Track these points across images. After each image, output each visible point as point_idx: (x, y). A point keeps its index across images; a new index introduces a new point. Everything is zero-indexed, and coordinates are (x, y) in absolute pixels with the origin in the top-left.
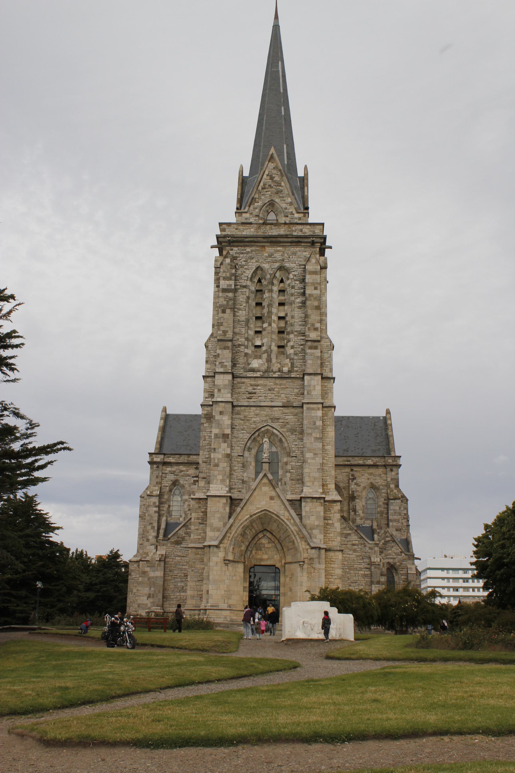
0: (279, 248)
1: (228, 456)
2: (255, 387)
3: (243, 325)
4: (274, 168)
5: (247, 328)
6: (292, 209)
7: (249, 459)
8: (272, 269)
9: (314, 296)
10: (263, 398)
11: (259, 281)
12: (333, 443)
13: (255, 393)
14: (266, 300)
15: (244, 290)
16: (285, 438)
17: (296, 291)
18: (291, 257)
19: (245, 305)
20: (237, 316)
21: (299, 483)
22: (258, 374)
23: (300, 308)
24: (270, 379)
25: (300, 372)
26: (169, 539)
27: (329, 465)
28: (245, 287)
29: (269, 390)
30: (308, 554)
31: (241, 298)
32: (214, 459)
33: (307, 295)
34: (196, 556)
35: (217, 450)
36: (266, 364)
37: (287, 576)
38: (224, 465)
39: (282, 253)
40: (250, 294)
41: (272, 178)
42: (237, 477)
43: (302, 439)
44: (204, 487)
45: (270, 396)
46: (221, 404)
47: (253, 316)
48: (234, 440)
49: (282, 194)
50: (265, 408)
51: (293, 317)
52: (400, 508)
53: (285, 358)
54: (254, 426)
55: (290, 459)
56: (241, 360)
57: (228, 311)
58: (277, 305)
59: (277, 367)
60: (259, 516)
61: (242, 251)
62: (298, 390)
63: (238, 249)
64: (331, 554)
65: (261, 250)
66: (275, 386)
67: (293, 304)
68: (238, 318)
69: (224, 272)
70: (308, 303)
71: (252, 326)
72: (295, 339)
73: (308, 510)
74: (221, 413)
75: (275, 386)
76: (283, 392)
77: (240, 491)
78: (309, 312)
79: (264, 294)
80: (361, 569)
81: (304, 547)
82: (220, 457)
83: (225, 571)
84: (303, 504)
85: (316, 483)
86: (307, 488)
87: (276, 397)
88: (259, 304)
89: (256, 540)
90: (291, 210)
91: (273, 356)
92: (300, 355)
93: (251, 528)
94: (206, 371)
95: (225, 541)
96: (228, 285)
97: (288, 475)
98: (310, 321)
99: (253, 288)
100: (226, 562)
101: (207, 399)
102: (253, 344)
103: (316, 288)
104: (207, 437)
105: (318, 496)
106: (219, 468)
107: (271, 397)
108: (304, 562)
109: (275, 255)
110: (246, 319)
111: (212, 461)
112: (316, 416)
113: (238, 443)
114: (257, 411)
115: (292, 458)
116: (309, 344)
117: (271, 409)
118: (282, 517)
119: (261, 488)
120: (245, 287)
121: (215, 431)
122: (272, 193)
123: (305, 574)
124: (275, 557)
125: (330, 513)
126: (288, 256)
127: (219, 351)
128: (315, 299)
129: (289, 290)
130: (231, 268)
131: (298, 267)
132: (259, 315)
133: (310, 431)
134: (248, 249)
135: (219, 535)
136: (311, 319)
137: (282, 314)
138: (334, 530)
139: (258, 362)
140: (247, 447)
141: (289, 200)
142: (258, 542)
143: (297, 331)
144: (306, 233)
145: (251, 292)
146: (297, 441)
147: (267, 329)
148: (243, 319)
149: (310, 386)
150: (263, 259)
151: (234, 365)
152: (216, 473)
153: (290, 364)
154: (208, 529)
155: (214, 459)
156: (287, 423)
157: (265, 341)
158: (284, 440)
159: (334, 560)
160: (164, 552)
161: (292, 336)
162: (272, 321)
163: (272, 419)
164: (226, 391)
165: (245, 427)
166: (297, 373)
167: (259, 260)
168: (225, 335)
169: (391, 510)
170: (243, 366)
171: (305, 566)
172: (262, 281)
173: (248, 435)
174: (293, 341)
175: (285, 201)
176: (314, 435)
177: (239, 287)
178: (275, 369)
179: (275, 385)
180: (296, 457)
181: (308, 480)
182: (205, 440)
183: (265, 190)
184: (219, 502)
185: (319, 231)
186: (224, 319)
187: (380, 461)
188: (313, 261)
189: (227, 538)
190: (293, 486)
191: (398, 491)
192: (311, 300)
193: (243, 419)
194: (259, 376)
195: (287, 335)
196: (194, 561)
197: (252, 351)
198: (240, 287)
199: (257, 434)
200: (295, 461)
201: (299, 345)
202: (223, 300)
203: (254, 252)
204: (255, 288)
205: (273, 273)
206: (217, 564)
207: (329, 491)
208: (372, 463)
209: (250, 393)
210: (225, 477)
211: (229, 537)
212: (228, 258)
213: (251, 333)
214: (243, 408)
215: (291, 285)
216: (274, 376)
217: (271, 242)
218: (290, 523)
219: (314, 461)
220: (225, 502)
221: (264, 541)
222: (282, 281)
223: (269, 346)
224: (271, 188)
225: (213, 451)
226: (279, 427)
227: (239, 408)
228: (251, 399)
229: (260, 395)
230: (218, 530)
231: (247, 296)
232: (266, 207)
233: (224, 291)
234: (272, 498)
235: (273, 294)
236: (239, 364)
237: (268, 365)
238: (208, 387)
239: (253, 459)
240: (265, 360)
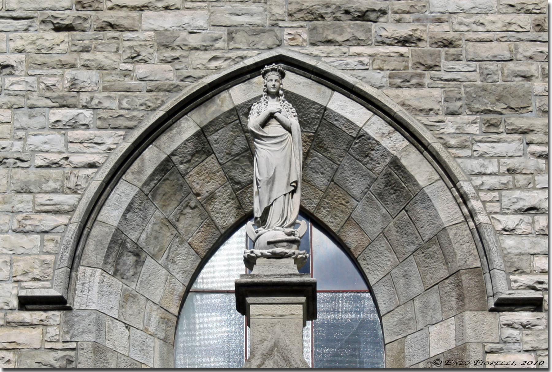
16: (436, 158)
156: (449, 44)
200: (530, 341)
226: (379, 77)
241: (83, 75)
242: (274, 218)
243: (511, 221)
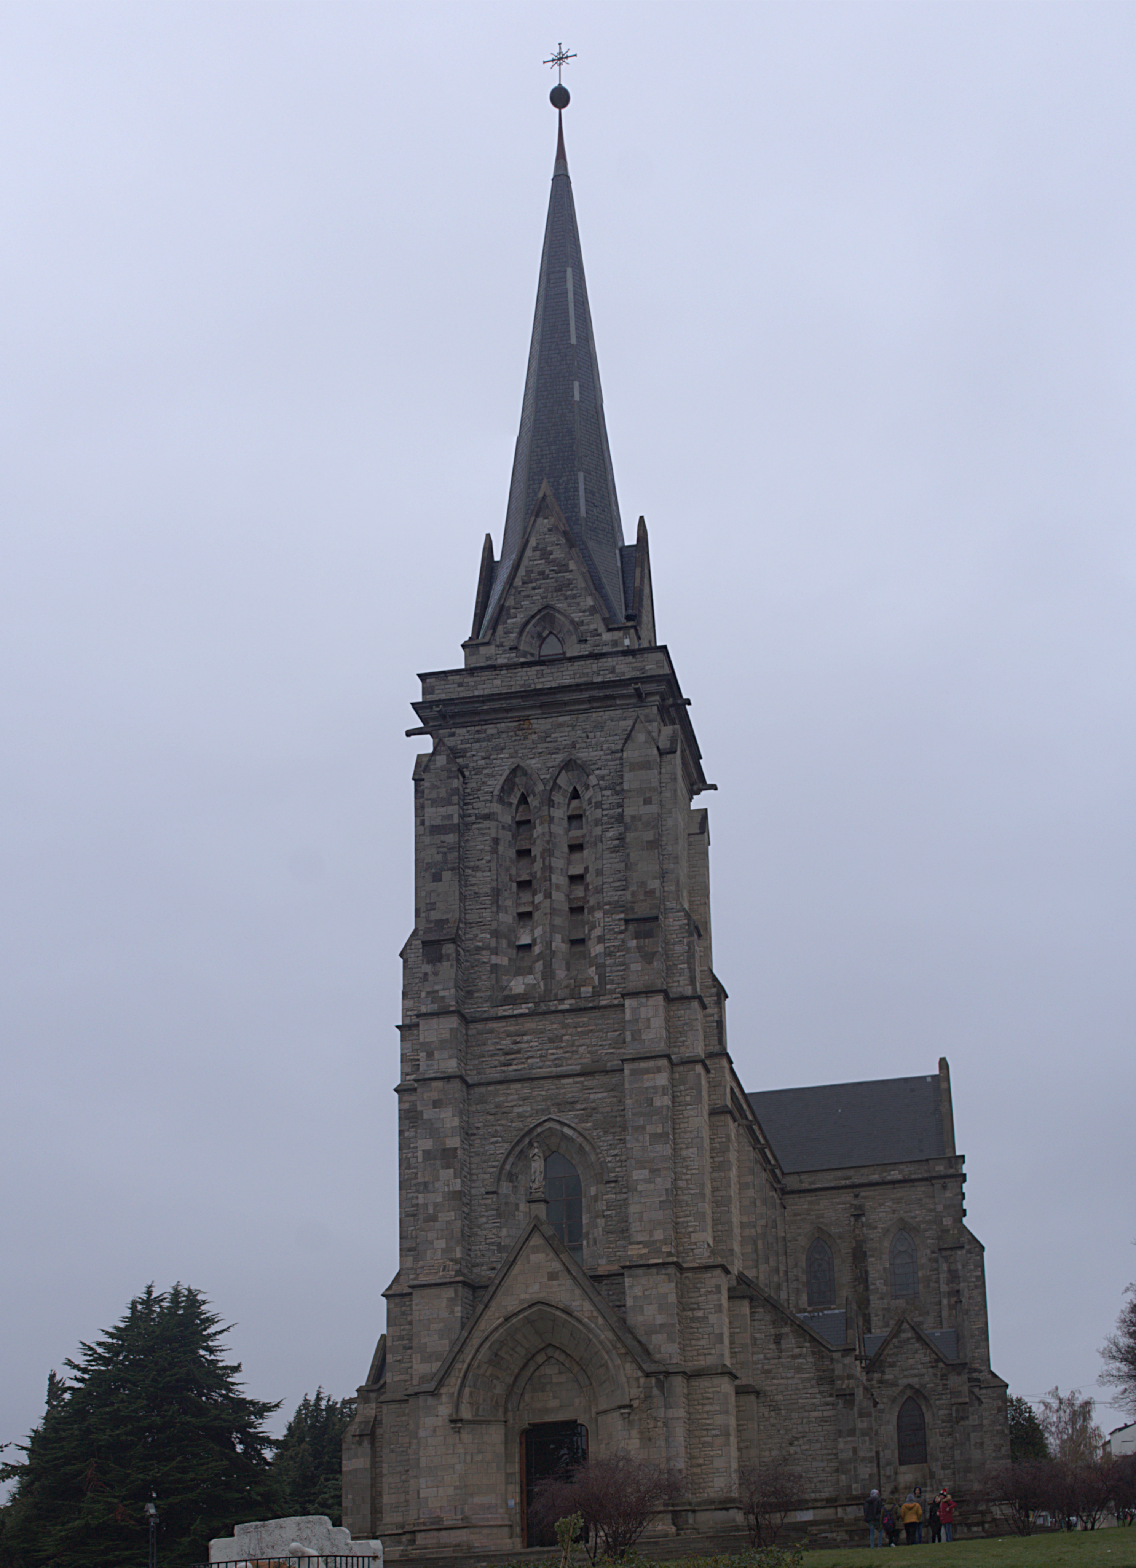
0: (561, 719)
1: (457, 1196)
2: (518, 1039)
5: (494, 909)
8: (549, 768)
10: (538, 1060)
11: (523, 799)
13: (518, 1052)
14: (538, 842)
15: (487, 823)
18: (591, 735)
19: (488, 858)
20: (471, 885)
22: (524, 1009)
24: (552, 1017)
27: (692, 1192)
28: (487, 817)
29: (551, 1040)
31: (479, 844)
38: (447, 1216)
40: (500, 831)
42: (486, 1239)
43: (623, 1141)
44: (412, 1268)
45: (553, 1054)
47: (511, 880)
48: (476, 1159)
50: (542, 1082)
54: (520, 1125)
56: (484, 982)
57: (447, 875)
62: (617, 1033)
64: (704, 1383)
66: (563, 1032)
68: (475, 888)
71: (509, 903)
72: (607, 920)
75: (563, 1032)
76: (582, 1042)
79: (535, 828)
84: (628, 1281)
86: (636, 1246)
87: (567, 1055)
88: (524, 853)
89: (532, 1369)
92: (618, 954)
94: (404, 1016)
96: (444, 818)
99: (507, 819)
101: (408, 1078)
102: (510, 944)
105: (660, 1261)
107: (553, 1057)
109: (553, 736)
110: (493, 889)
112: (655, 1087)
113: (484, 1165)
114: (525, 1090)
115: (608, 1185)
117: (557, 1082)
120: (487, 817)
124: (577, 1401)
126: (584, 735)
130: (449, 778)
131: (609, 757)
132: (525, 877)
133: (641, 1121)
139: (526, 981)
142: (537, 1374)
143: (608, 904)
145: (503, 828)
146: (619, 1146)
148: (487, 889)
149: (637, 1021)
150: (525, 748)
153: (596, 978)
156: (594, 1109)
157: (538, 932)
158: (587, 1148)
159: (711, 1396)
161: (599, 915)
162: (554, 887)
163: (558, 1104)
166: (614, 996)
167: (516, 752)
170: (489, 993)
172: (529, 800)
173: (506, 1145)
174: (602, 925)
176: (650, 1129)
177: (473, 818)
179: (563, 1028)
180: (616, 1181)
181: (639, 1229)
186: (438, 895)
193: (493, 1111)
194: (527, 1011)
195: (589, 914)
197: (510, 959)
199: (527, 1140)
201: (616, 933)
203: (504, 735)
204: (513, 818)
209: (507, 1054)
213: (507, 919)
214: (491, 1088)
216: (561, 1007)
217: (542, 706)
218: (596, 1324)
219: (651, 1186)
221: (549, 1370)
223: (547, 943)
226: (576, 1120)
227: (483, 1089)
228: (510, 1065)
233: (435, 830)
235: (552, 826)
236: (479, 991)
237: (546, 985)
238: (410, 1050)
240: (539, 976)
241: (498, 1128)
243: (609, 1159)
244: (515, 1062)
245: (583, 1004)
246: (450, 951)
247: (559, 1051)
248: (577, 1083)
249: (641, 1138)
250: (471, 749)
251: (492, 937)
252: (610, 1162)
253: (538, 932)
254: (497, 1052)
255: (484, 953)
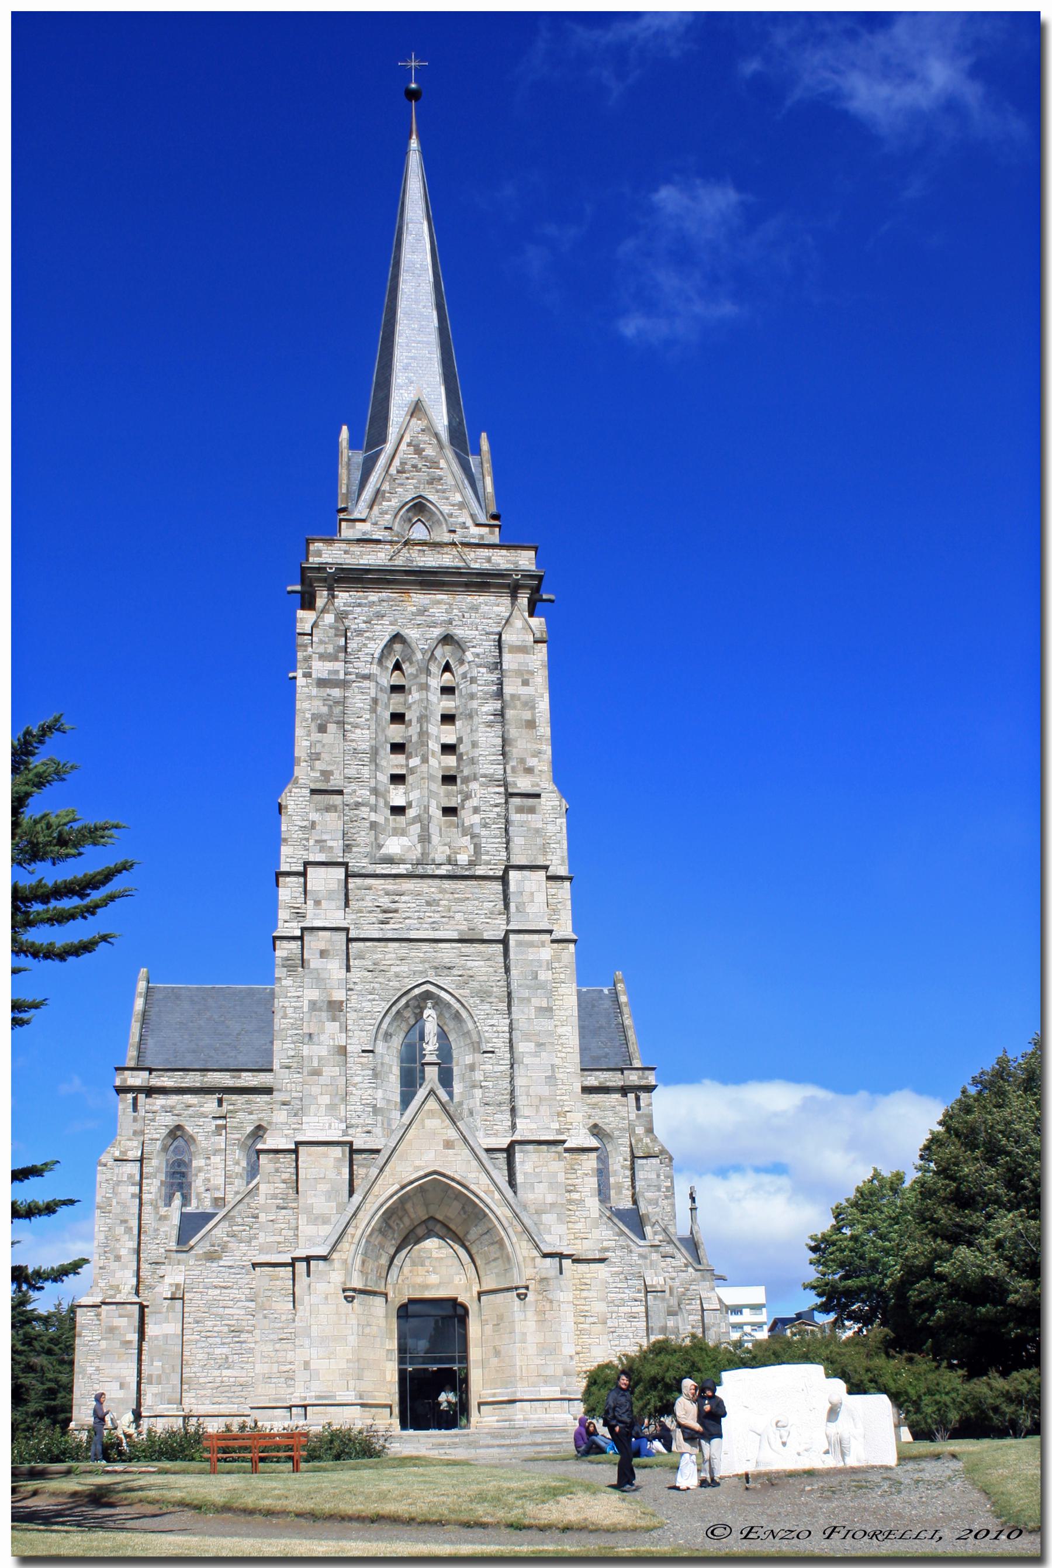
0: (439, 597)
2: (397, 898)
3: (366, 759)
4: (423, 430)
5: (373, 767)
6: (465, 518)
7: (387, 1059)
9: (523, 698)
10: (416, 921)
11: (397, 667)
12: (575, 1021)
13: (396, 911)
14: (414, 707)
15: (366, 684)
16: (468, 1010)
17: (480, 688)
19: (368, 717)
21: (502, 1112)
22: (402, 869)
23: (490, 725)
24: (430, 881)
25: (495, 864)
26: (192, 1248)
27: (568, 1071)
28: (367, 677)
29: (428, 904)
30: (535, 1270)
32: (311, 1057)
33: (507, 697)
34: (272, 1283)
35: (315, 1039)
36: (419, 846)
37: (487, 1321)
39: (447, 606)
41: (418, 451)
42: (361, 1099)
45: (430, 917)
46: (321, 933)
47: (386, 741)
49: (442, 485)
51: (474, 745)
52: (658, 1176)
53: (460, 835)
55: (479, 1057)
56: (363, 837)
57: (332, 728)
58: (439, 718)
59: (443, 853)
60: (420, 1185)
61: (359, 601)
62: (493, 904)
63: (350, 596)
65: (402, 599)
66: (441, 896)
67: (475, 717)
69: (321, 642)
70: (510, 713)
72: (483, 792)
73: (530, 1171)
74: (323, 954)
75: (441, 896)
77: (369, 1132)
78: (513, 732)
79: (410, 693)
80: (623, 1303)
81: (525, 1253)
82: (324, 1053)
83: (347, 1314)
84: (518, 1157)
85: (544, 1109)
88: (398, 718)
90: (461, 520)
91: (434, 829)
92: (493, 826)
93: (400, 1213)
95: (344, 1245)
97: (478, 1092)
98: (515, 752)
100: (350, 1294)
102: (386, 803)
103: (526, 683)
104: (290, 1011)
106: (322, 1080)
108: (527, 1288)
109: (431, 610)
111: (306, 1063)
112: (539, 961)
113: (361, 1022)
114: (402, 949)
116: (516, 801)
117: (434, 945)
118: (472, 1187)
119: (423, 1120)
120: (367, 677)
121: (312, 994)
122: (419, 482)
123: (530, 1314)
124: (456, 1279)
125: (574, 1176)
127: (314, 816)
128: (525, 704)
129: (463, 687)
130: (336, 635)
132: (398, 740)
133: (526, 993)
134: (373, 597)
135: (327, 1232)
136: (517, 747)
137: (451, 740)
138: (585, 1214)
140: (382, 1031)
141: (458, 498)
143: (485, 776)
144: (499, 565)
145: (381, 690)
146: (495, 1017)
147: (418, 770)
148: (365, 746)
149: (521, 893)
150: (404, 618)
151: (347, 848)
152: (315, 1090)
154: (303, 1219)
155: (311, 1057)
157: (414, 796)
158: (464, 1014)
159: (588, 1281)
160: (180, 1279)
161: (474, 786)
162: (430, 754)
164: (333, 905)
165: (377, 986)
166: (490, 867)
167: (396, 620)
168: (327, 780)
169: (641, 1180)
171: (531, 1297)
172: (404, 667)
173: (383, 1004)
175: (447, 499)
176: (536, 1002)
178: (440, 857)
179: (440, 892)
180: (493, 1052)
182: (285, 1017)
183: (405, 475)
184: (326, 1156)
185: (527, 563)
186: (323, 746)
187: (614, 1079)
188: (518, 623)
189: (347, 1238)
190: (489, 1118)
191: (652, 1140)
192: (515, 708)
193: (371, 968)
194: (405, 872)
195: (462, 783)
196: (269, 1293)
198: (357, 677)
199: (403, 1001)
200: (491, 1062)
202: (320, 703)
203: (385, 604)
204: (388, 681)
205: (429, 648)
206: (326, 1298)
207: (570, 1127)
208: (596, 1083)
209: (385, 912)
210: (337, 1101)
211: (353, 1236)
212: (328, 613)
213: (384, 778)
215: (469, 676)
216: (438, 872)
218: (493, 1199)
220: (341, 1156)
222: (447, 668)
223: (425, 807)
224: (417, 471)
225: (306, 1039)
228: (388, 923)
229: (407, 914)
230: (326, 1221)
231: (373, 698)
232: (408, 511)
234: (448, 1145)
236: (358, 846)
237: (423, 848)
239: (395, 1059)
240: (416, 839)
241: (377, 986)
242: (430, 1043)
243: (487, 1028)
244: (392, 921)
245: (460, 872)
246: (336, 803)
247: (437, 915)
248: (453, 948)
249: (526, 1010)
250: (352, 612)
251: (371, 794)
252: (487, 1031)
253: (414, 796)
254: (376, 909)
255: (363, 809)
